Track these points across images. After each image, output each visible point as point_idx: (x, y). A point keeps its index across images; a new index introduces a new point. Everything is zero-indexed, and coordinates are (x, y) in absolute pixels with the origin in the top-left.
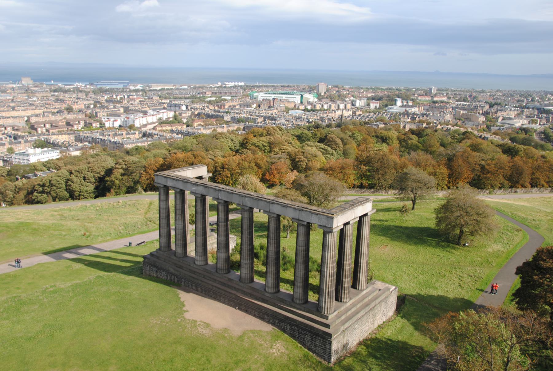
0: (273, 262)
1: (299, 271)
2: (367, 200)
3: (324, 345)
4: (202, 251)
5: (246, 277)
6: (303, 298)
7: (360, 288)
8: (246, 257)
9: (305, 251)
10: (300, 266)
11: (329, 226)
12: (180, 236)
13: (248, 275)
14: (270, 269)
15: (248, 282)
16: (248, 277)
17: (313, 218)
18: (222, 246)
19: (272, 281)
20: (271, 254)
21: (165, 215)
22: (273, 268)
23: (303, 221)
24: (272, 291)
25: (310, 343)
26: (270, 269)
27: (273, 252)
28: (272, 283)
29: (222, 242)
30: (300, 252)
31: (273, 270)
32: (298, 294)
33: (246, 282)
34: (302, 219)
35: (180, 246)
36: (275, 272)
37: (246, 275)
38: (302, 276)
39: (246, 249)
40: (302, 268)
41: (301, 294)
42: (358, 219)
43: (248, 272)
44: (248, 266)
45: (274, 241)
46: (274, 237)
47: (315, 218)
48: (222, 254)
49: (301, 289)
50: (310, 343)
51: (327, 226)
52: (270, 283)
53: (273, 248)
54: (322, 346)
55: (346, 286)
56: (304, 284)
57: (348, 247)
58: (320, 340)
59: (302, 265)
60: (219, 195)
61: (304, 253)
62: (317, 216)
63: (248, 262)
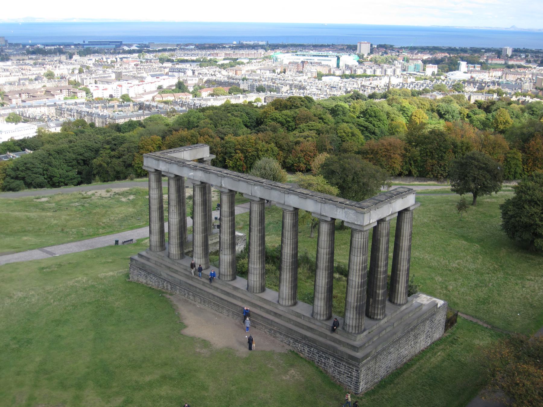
0: (288, 267)
1: (321, 279)
2: (410, 191)
3: (350, 372)
5: (255, 286)
6: (325, 313)
7: (399, 302)
8: (255, 260)
9: (329, 254)
10: (321, 273)
11: (359, 223)
12: (174, 232)
14: (285, 276)
15: (258, 291)
16: (258, 286)
17: (338, 213)
18: (226, 246)
19: (287, 291)
20: (286, 257)
21: (156, 207)
22: (288, 275)
23: (326, 216)
24: (287, 304)
25: (333, 369)
26: (285, 276)
27: (288, 255)
28: (287, 294)
29: (226, 241)
30: (322, 255)
32: (319, 308)
33: (255, 291)
34: (324, 214)
35: (174, 246)
36: (290, 279)
37: (255, 283)
38: (323, 286)
39: (256, 250)
40: (324, 275)
41: (322, 308)
42: (397, 215)
43: (258, 279)
45: (289, 240)
46: (289, 235)
47: (341, 212)
48: (226, 256)
49: (323, 301)
50: (333, 369)
51: (356, 223)
52: (284, 293)
54: (347, 374)
55: (380, 298)
56: (327, 295)
57: (383, 250)
58: (345, 366)
59: (324, 271)
60: (223, 182)
61: (328, 257)
62: (344, 211)
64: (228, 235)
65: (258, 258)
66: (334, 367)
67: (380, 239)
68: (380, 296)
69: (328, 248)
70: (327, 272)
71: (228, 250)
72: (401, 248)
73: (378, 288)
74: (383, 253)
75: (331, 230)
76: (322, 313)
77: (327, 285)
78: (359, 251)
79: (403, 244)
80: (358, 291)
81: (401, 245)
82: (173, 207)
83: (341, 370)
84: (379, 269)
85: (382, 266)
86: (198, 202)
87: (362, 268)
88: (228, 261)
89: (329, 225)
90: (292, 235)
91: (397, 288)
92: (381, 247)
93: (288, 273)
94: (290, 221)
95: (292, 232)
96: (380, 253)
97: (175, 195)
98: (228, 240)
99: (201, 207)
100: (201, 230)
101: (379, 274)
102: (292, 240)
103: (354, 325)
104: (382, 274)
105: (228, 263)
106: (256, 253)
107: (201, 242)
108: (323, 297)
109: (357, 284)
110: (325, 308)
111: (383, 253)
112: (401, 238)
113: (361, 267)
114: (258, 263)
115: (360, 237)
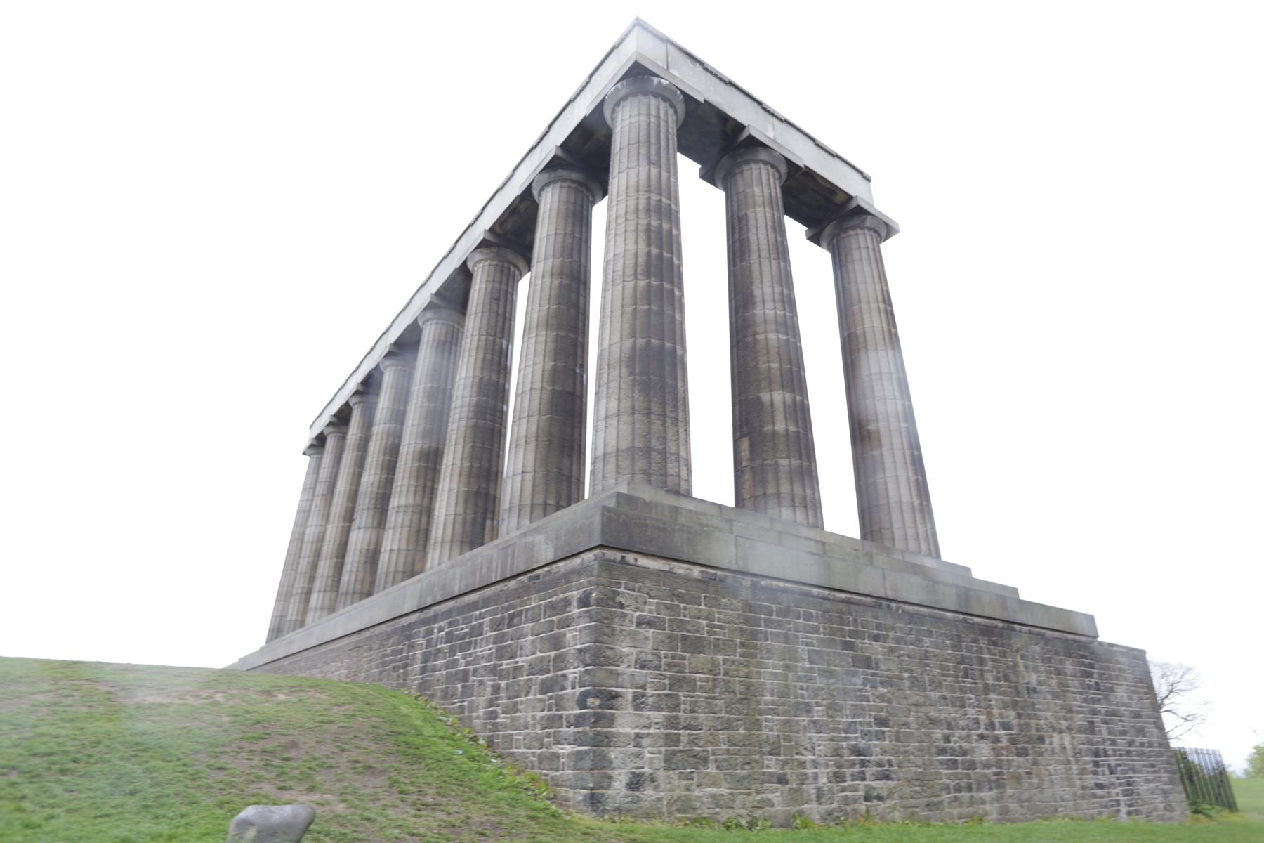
0: (463, 423)
4: (332, 570)
13: (402, 560)
22: (460, 447)
27: (470, 381)
31: (459, 455)
32: (519, 478)
36: (467, 464)
38: (538, 385)
40: (541, 347)
41: (529, 477)
44: (408, 518)
45: (476, 338)
48: (362, 531)
49: (532, 447)
53: (472, 366)
55: (780, 427)
56: (551, 420)
61: (556, 282)
63: (411, 501)
64: (379, 472)
65: (414, 474)
66: (494, 671)
67: (746, 215)
68: (779, 416)
69: (558, 254)
70: (552, 334)
71: (371, 513)
72: (861, 339)
73: (764, 384)
74: (764, 253)
75: (571, 207)
76: (527, 500)
77: (553, 383)
78: (634, 152)
79: (867, 325)
80: (635, 287)
81: (859, 332)
82: (320, 498)
83: (520, 661)
84: (758, 311)
85: (768, 297)
86: (353, 441)
87: (649, 204)
88: (365, 547)
89: (565, 190)
90: (485, 322)
91: (881, 488)
92: (752, 237)
93: (461, 441)
94: (483, 286)
95: (486, 315)
96: (754, 255)
97: (330, 470)
98: (376, 485)
99: (355, 453)
100: (343, 511)
101: (760, 329)
102: (484, 338)
103: (625, 444)
104: (771, 327)
105: (364, 552)
106: (410, 457)
107: (337, 542)
108: (534, 428)
109: (631, 261)
110: (539, 475)
111: (764, 253)
112: (856, 308)
113: (642, 202)
114: (412, 489)
115: (635, 112)
